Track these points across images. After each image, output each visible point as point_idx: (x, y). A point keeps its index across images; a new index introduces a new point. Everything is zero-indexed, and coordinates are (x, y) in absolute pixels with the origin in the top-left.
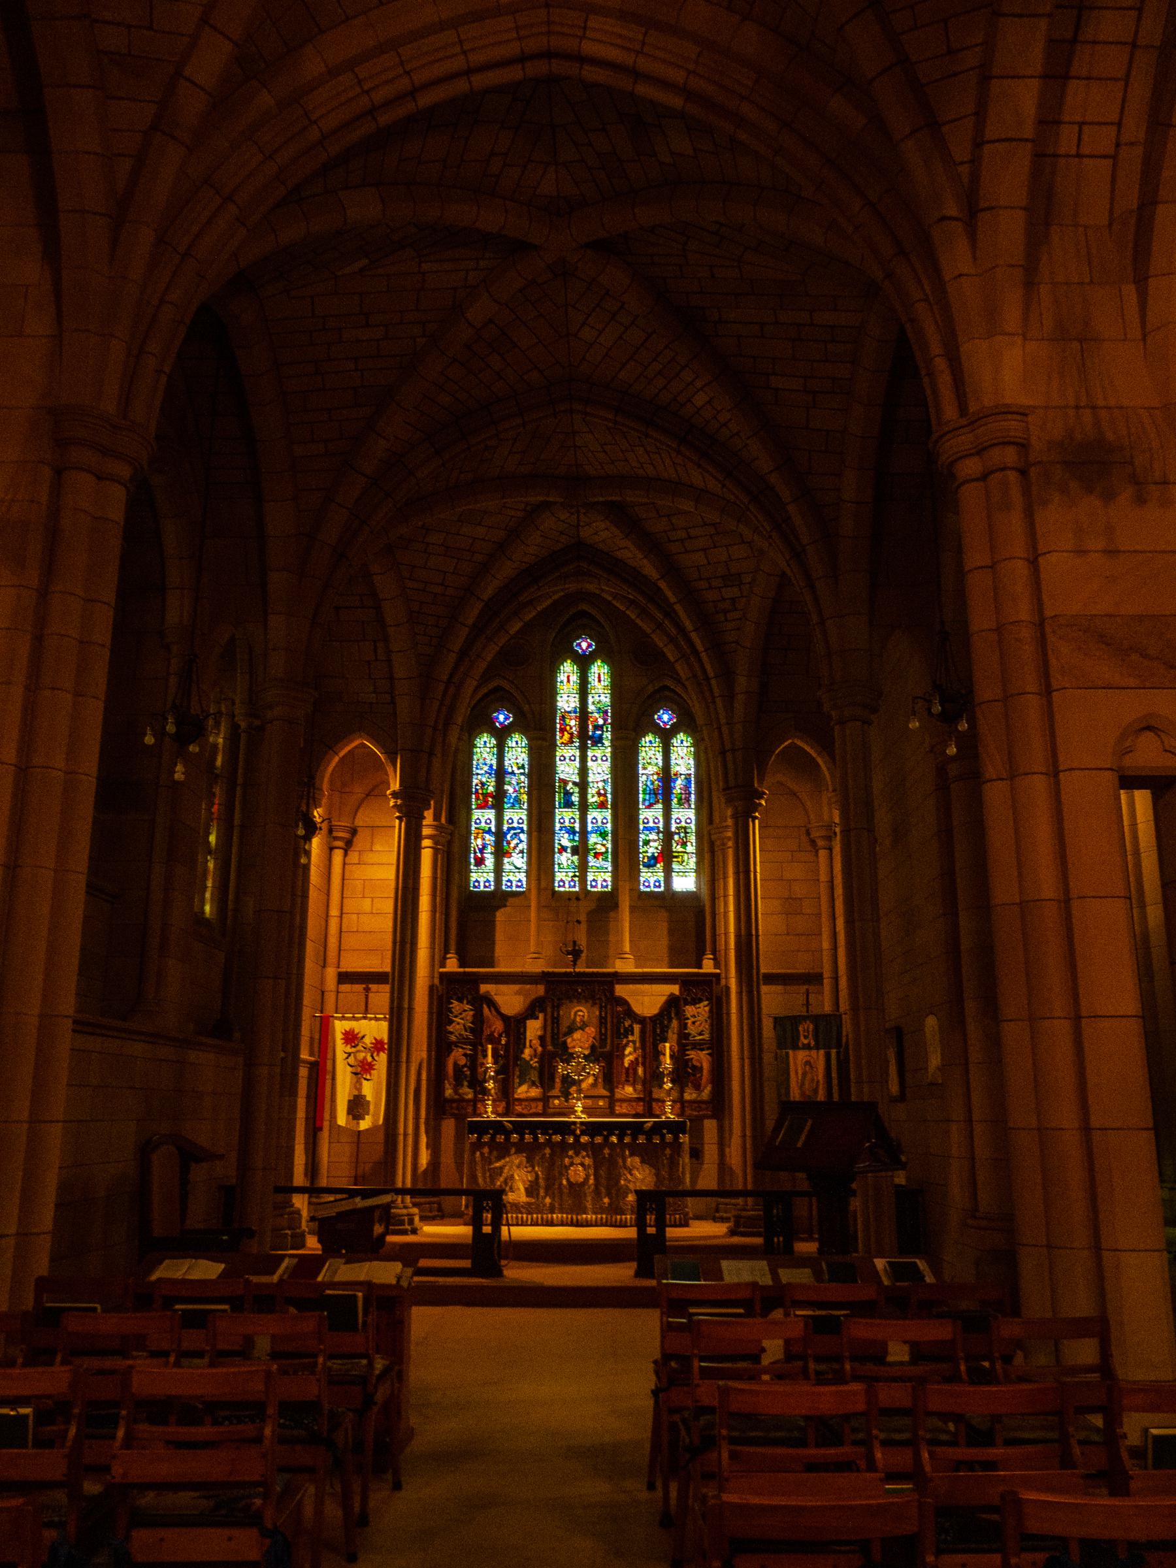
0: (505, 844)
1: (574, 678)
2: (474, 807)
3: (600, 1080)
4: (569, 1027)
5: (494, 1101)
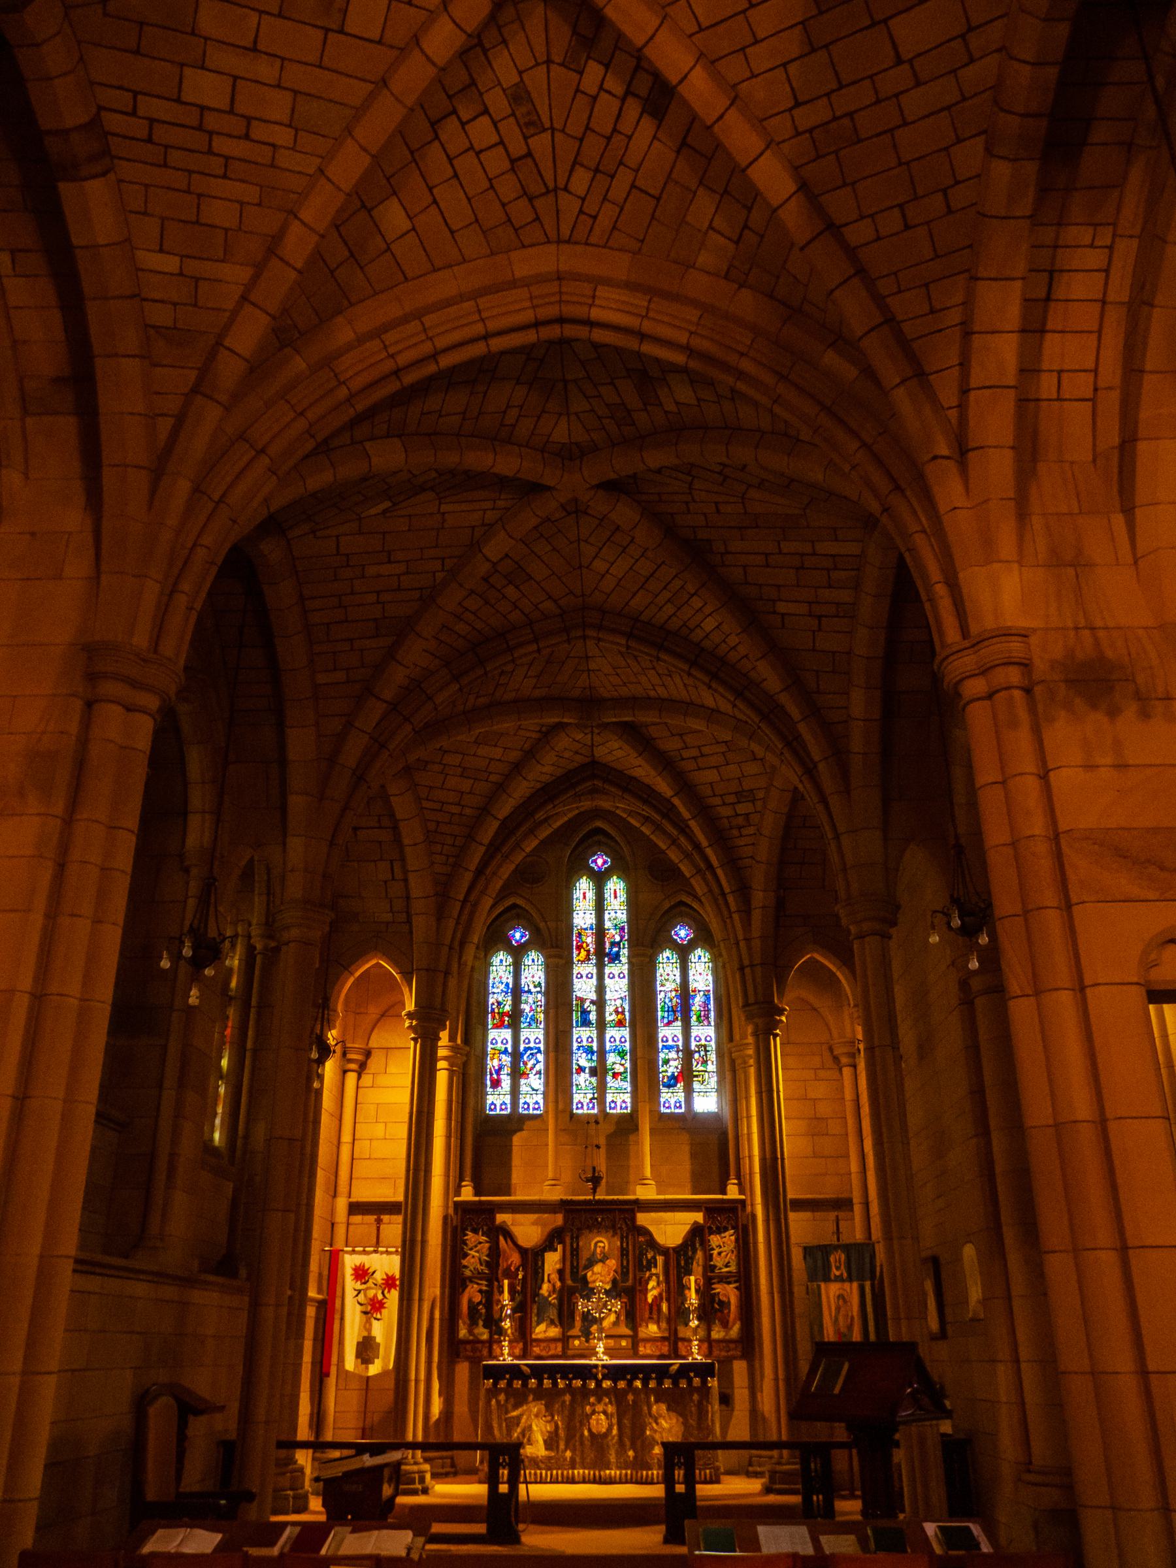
1: (591, 895)
2: (490, 1027)
4: (588, 1259)
5: (510, 1342)
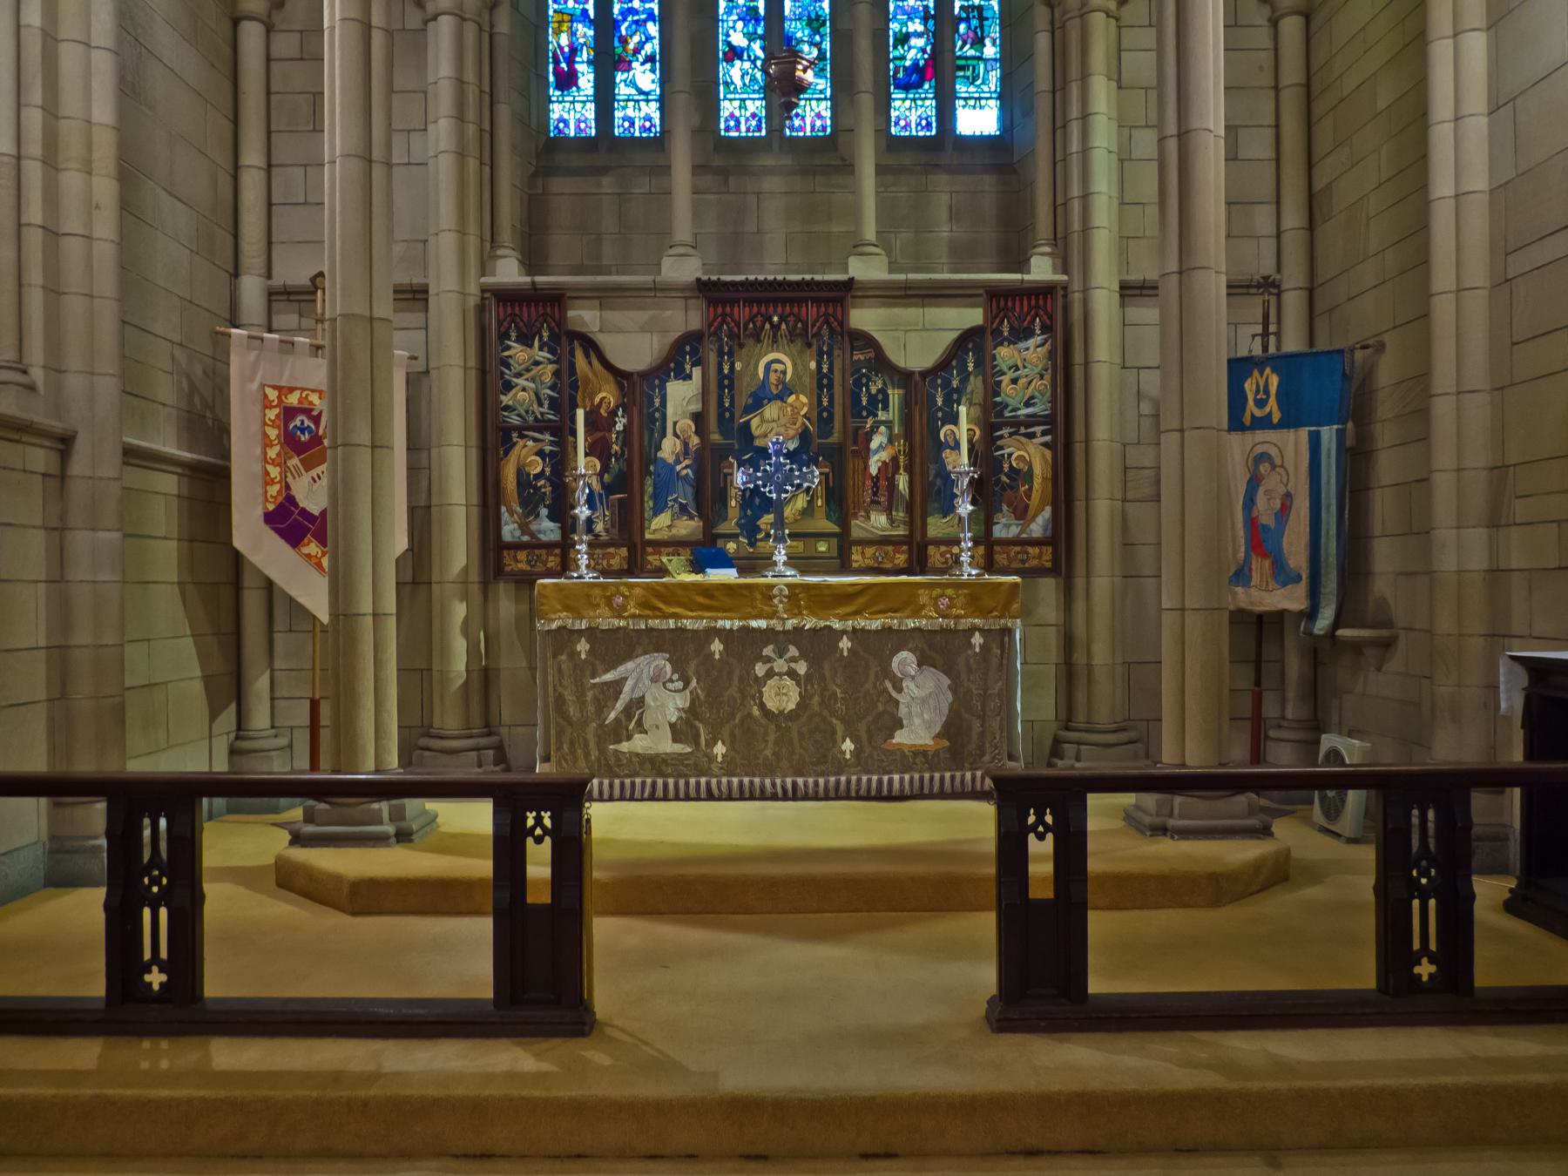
0: (616, 43)
3: (820, 503)
4: (753, 395)
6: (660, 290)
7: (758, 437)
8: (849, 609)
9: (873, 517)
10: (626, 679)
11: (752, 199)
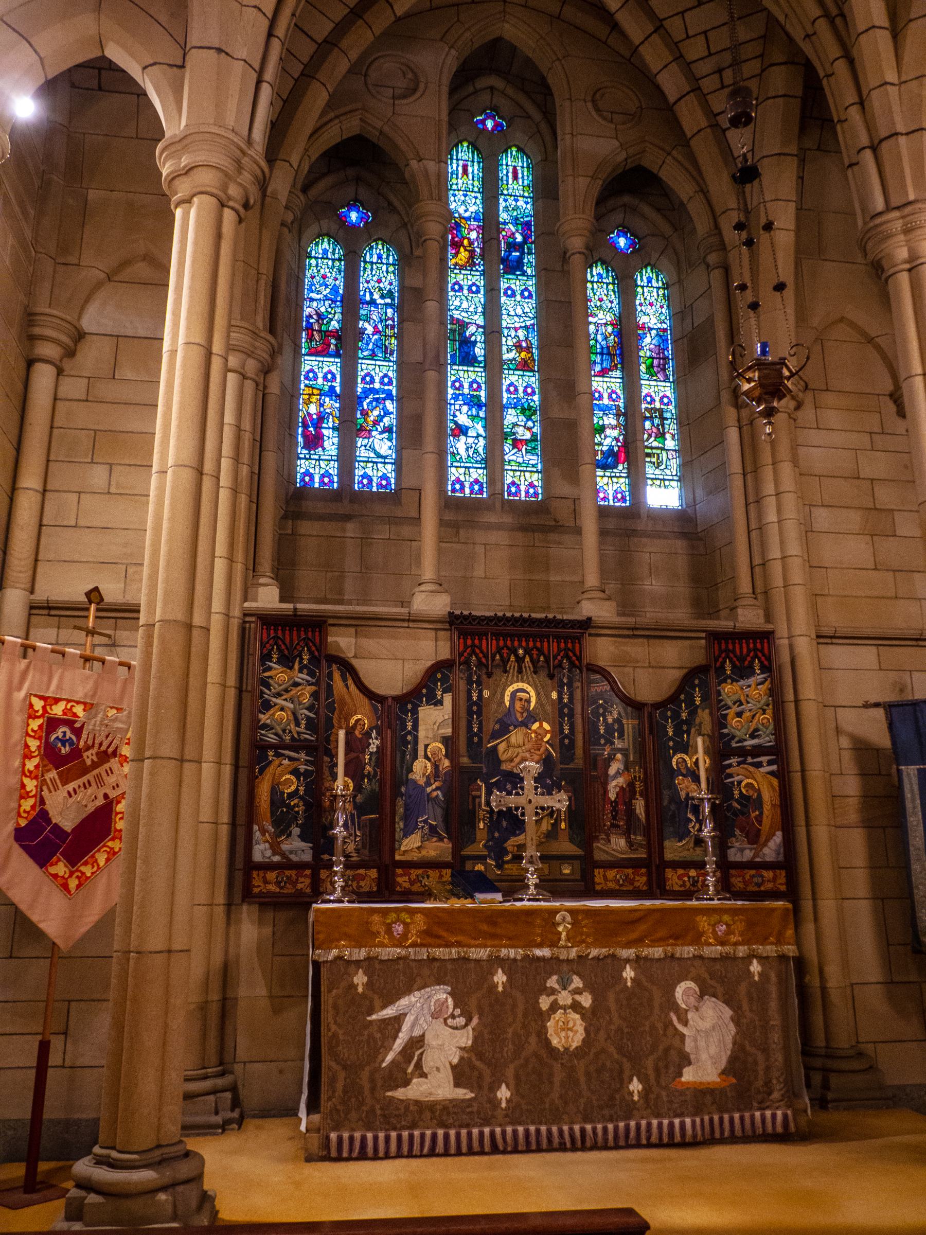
0: (359, 416)
1: (475, 168)
2: (303, 351)
3: (563, 826)
6: (413, 620)
7: (505, 761)
8: (634, 936)
9: (613, 840)
10: (405, 1015)
11: (480, 550)
